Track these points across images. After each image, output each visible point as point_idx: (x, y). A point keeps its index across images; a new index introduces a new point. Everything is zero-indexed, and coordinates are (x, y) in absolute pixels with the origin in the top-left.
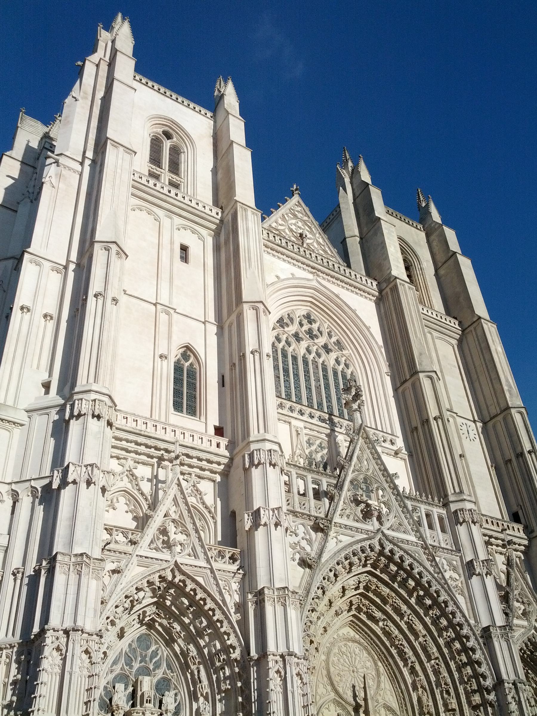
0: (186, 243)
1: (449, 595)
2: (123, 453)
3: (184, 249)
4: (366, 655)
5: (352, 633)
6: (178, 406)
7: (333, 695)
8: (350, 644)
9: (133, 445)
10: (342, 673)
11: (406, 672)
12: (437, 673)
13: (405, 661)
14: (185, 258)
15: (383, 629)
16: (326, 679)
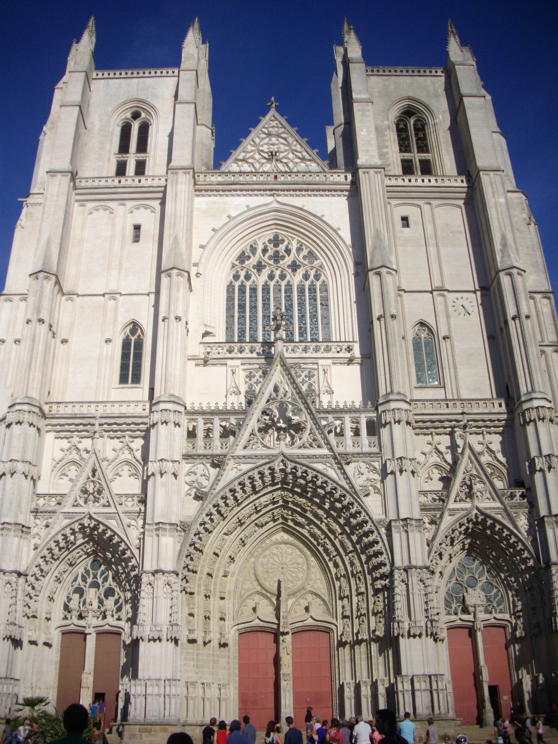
0: (137, 222)
1: (354, 498)
2: (69, 433)
3: (137, 228)
4: (298, 552)
6: (123, 379)
7: (259, 588)
8: (282, 546)
9: (73, 426)
10: (270, 571)
11: (331, 564)
12: (352, 564)
13: (328, 554)
14: (137, 238)
15: (309, 531)
16: (253, 577)
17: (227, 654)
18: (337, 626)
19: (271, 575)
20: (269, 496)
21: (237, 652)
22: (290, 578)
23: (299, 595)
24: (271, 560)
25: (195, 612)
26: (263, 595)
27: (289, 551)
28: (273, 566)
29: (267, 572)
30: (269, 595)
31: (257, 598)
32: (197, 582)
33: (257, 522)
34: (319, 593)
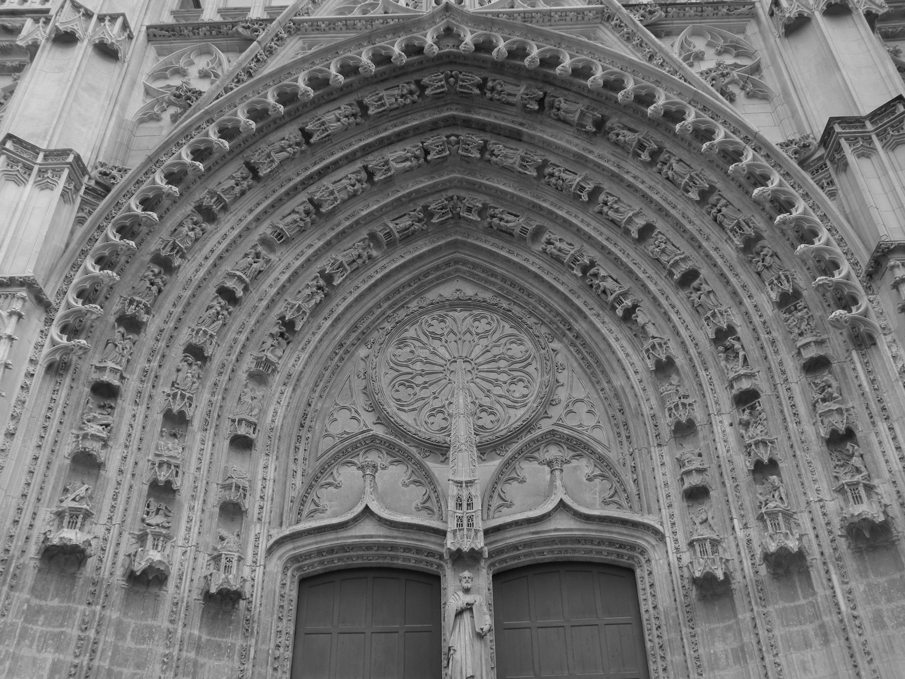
5: (469, 291)
7: (379, 431)
8: (459, 315)
16: (361, 401)
17: (239, 642)
18: (660, 536)
19: (424, 393)
20: (410, 148)
21: (287, 640)
22: (486, 401)
23: (515, 447)
24: (424, 353)
25: (113, 458)
26: (390, 448)
27: (482, 326)
28: (428, 368)
29: (408, 384)
30: (413, 450)
31: (373, 457)
32: (141, 364)
33: (376, 228)
34: (585, 438)
